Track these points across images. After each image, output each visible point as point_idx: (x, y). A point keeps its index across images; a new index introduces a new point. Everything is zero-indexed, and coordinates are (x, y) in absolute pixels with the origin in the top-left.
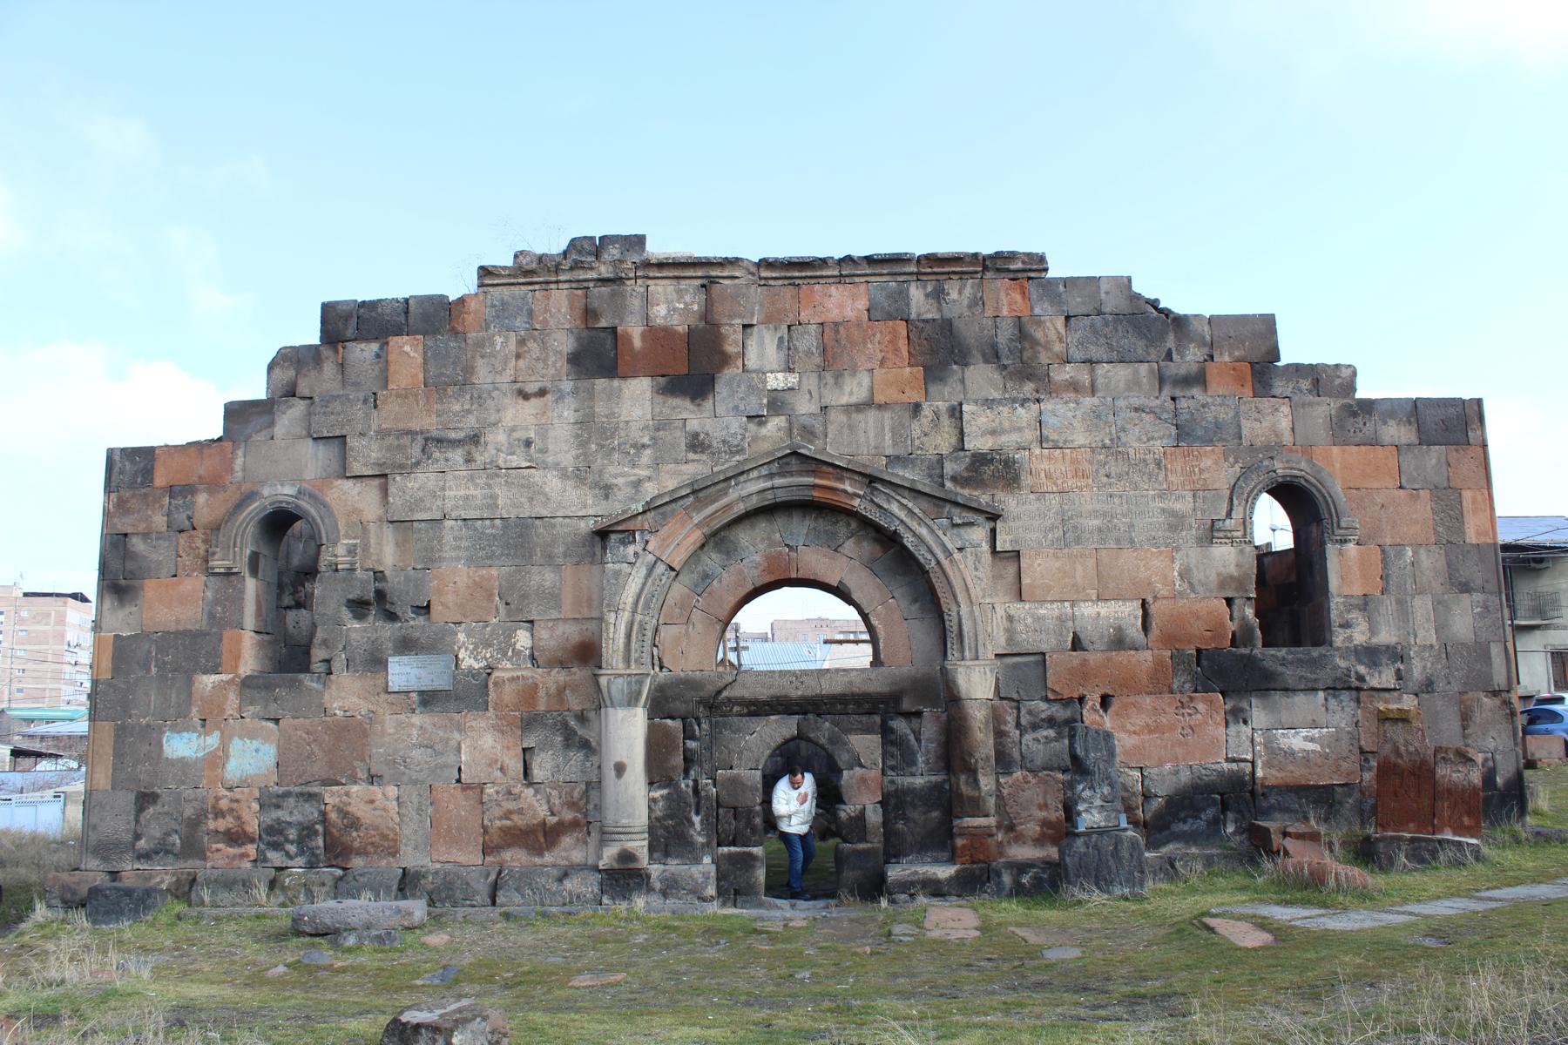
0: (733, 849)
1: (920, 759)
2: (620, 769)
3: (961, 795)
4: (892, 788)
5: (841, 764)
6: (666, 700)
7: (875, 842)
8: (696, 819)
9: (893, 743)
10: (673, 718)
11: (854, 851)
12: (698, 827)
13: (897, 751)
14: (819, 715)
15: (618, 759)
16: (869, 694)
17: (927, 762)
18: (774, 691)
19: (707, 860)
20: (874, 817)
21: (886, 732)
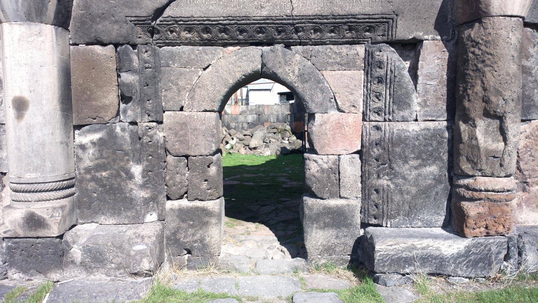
0: (185, 203)
1: (416, 100)
2: (20, 105)
3: (478, 147)
4: (376, 136)
5: (312, 106)
6: (93, 20)
7: (351, 200)
8: (137, 170)
9: (380, 80)
10: (104, 45)
11: (325, 208)
12: (138, 178)
13: (384, 92)
14: (288, 46)
15: (18, 94)
16: (354, 16)
17: (424, 104)
18: (231, 11)
19: (152, 217)
20: (351, 170)
21: (370, 64)
